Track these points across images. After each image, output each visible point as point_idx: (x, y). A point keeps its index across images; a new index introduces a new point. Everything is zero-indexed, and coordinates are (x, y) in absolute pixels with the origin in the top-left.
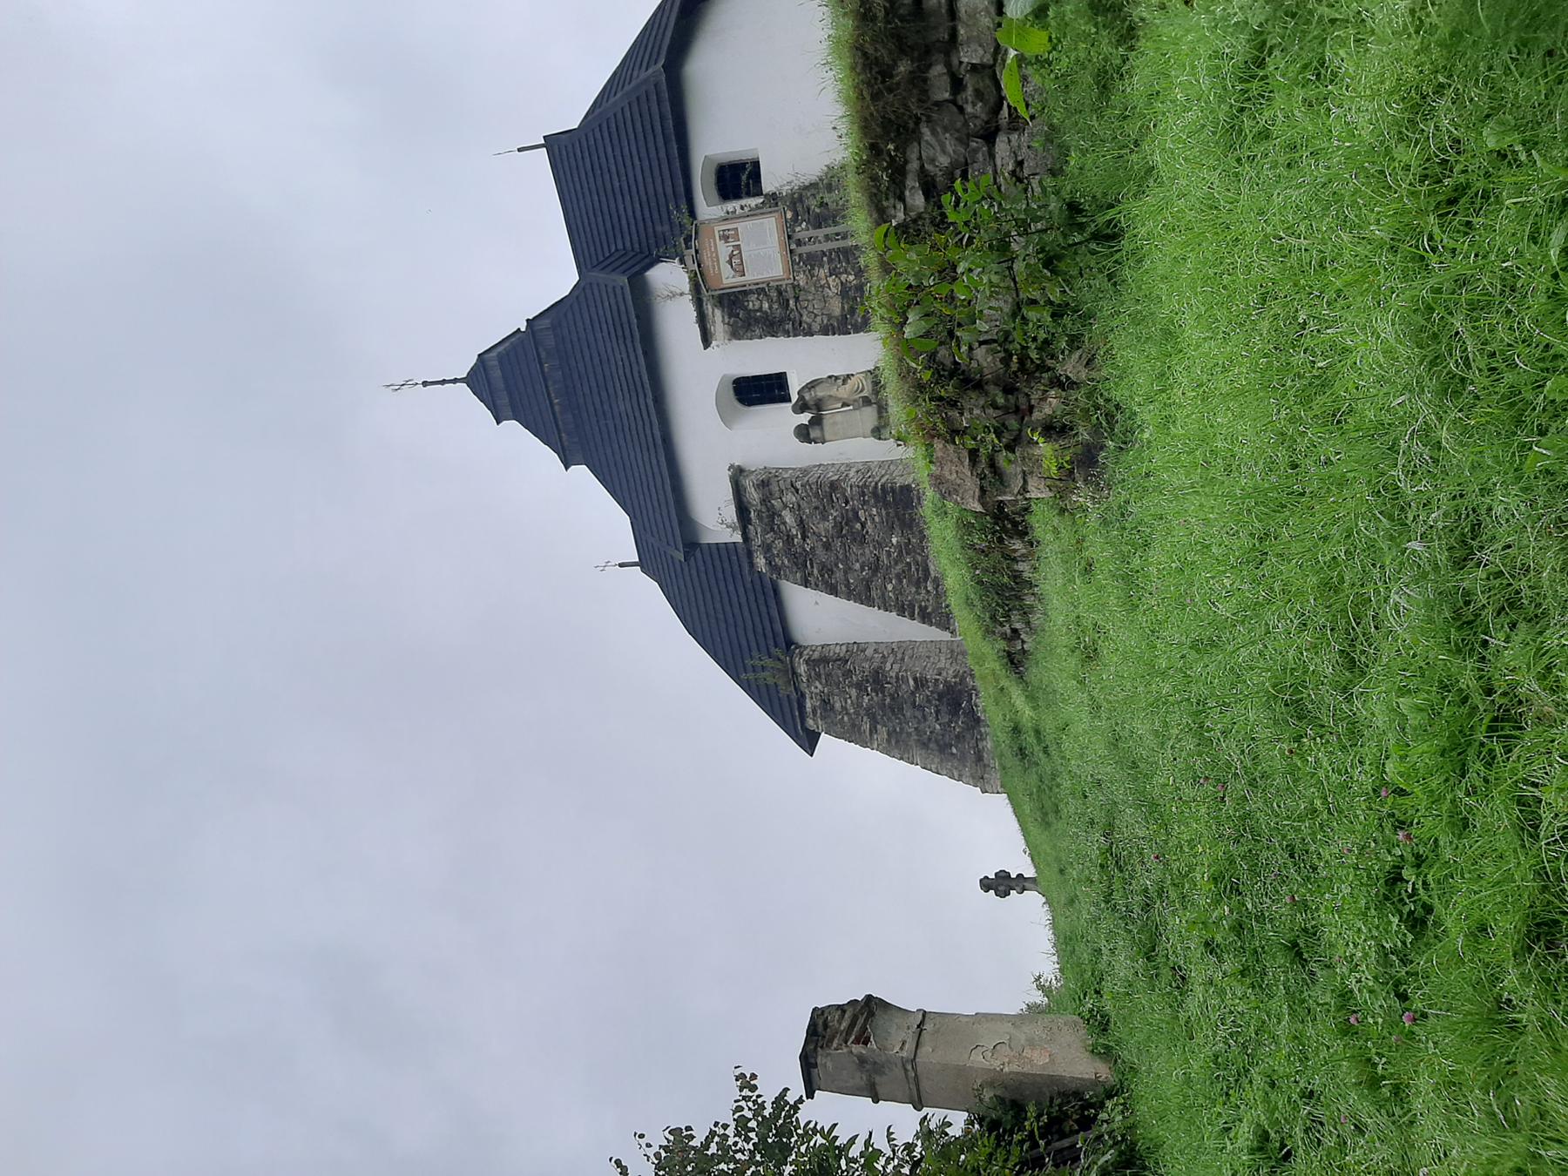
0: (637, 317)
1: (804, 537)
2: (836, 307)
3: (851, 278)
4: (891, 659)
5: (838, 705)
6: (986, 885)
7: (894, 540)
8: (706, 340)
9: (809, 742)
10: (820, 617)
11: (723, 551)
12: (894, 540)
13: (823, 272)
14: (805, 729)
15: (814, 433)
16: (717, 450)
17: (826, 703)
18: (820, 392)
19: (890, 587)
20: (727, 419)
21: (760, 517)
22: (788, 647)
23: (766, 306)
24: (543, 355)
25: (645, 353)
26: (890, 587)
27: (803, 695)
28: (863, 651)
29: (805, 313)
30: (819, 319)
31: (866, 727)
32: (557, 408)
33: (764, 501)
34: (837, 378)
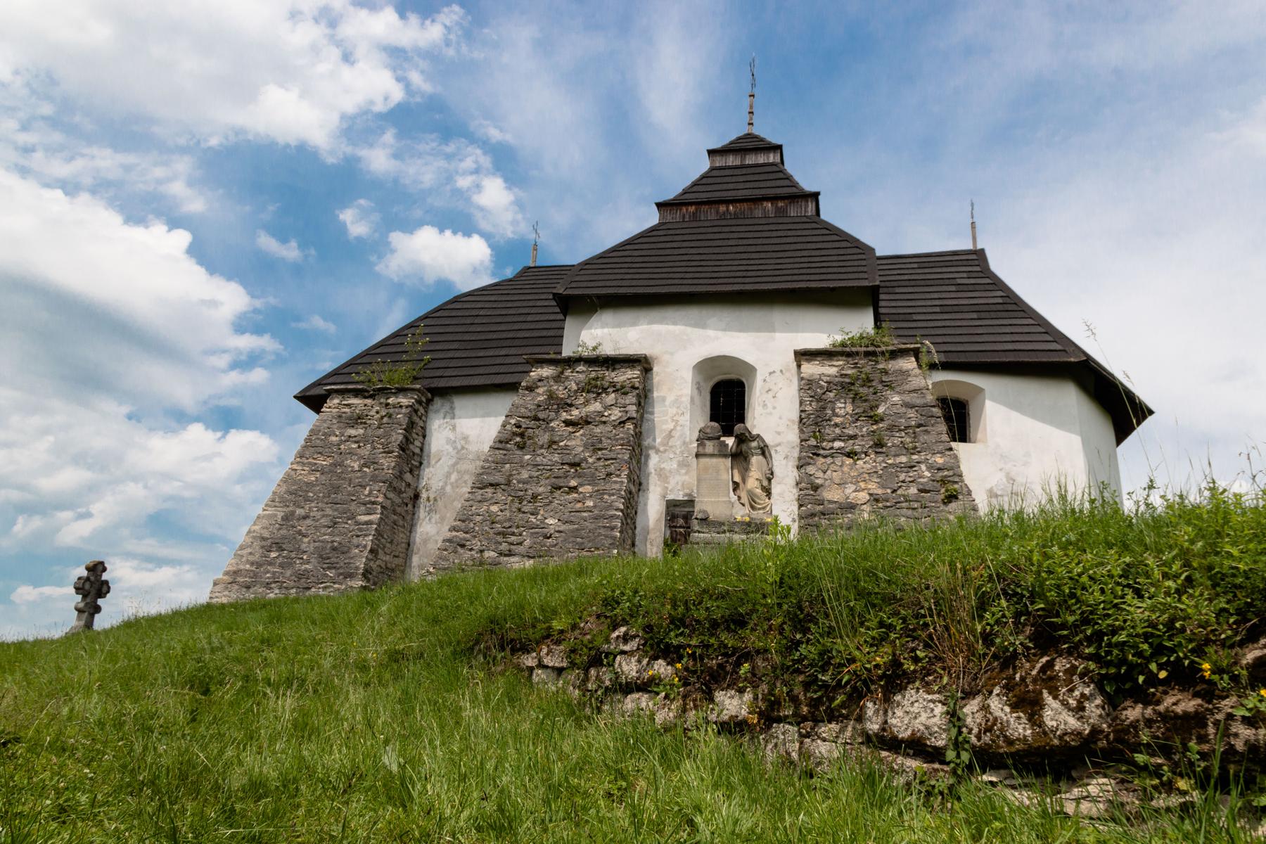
0: (833, 289)
1: (568, 423)
2: (832, 495)
3: (866, 515)
4: (398, 500)
5: (352, 432)
6: (97, 569)
7: (550, 521)
8: (803, 356)
9: (313, 399)
10: (467, 432)
11: (558, 341)
12: (550, 521)
13: (874, 487)
14: (330, 393)
15: (710, 447)
16: (678, 346)
17: (358, 420)
18: (756, 460)
19: (494, 508)
20: (707, 366)
21: (596, 379)
22: (430, 390)
23: (838, 420)
24: (780, 204)
25: (793, 291)
26: (494, 508)
27: (372, 397)
28: (411, 471)
29: (829, 460)
30: (820, 474)
31: (323, 462)
32: (722, 208)
33: (613, 385)
34: (769, 480)
